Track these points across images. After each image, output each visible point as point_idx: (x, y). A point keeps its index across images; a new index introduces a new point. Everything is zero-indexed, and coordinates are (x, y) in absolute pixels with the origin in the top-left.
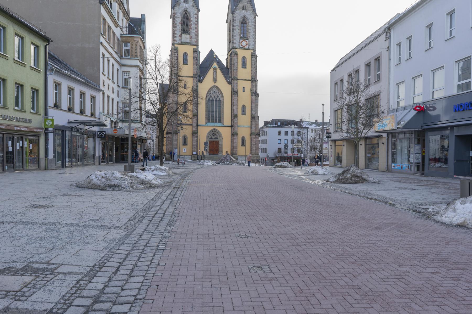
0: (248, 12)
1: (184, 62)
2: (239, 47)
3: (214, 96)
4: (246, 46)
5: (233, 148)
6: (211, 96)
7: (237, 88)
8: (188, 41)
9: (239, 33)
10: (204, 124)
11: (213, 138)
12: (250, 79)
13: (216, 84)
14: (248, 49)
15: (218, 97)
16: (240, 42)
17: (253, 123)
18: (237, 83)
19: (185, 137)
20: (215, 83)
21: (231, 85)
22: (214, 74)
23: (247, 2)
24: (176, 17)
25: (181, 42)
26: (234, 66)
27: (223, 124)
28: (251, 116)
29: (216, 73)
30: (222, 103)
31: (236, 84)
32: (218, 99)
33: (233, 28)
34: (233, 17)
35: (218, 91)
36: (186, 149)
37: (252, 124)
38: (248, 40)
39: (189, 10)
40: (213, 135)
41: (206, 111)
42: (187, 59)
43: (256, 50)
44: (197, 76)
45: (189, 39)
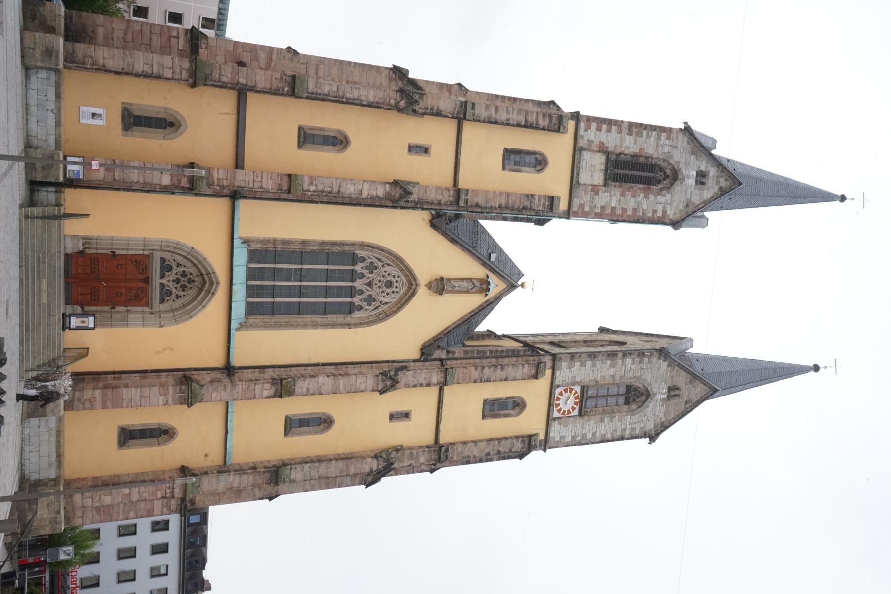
0: (663, 406)
1: (512, 157)
2: (557, 383)
3: (369, 284)
4: (559, 411)
5: (106, 387)
6: (372, 268)
7: (407, 386)
8: (584, 178)
9: (604, 377)
10: (241, 231)
11: (162, 276)
12: (443, 440)
13: (422, 291)
14: (549, 419)
15: (370, 300)
16: (574, 384)
17: (251, 477)
18: (428, 385)
19: (172, 124)
20: (429, 286)
21: (417, 356)
22: (465, 284)
24: (659, 138)
25: (582, 149)
26: (495, 366)
27: (242, 326)
28: (284, 465)
29: (467, 291)
30: (340, 318)
31: (424, 382)
32: (357, 300)
33: (620, 355)
34: (652, 355)
35: (392, 299)
36: (97, 122)
37: (240, 470)
38: (580, 414)
39: (677, 187)
40: (184, 274)
41: (304, 242)
42: (523, 169)
43: (545, 451)
44: (462, 204)
45: (588, 181)
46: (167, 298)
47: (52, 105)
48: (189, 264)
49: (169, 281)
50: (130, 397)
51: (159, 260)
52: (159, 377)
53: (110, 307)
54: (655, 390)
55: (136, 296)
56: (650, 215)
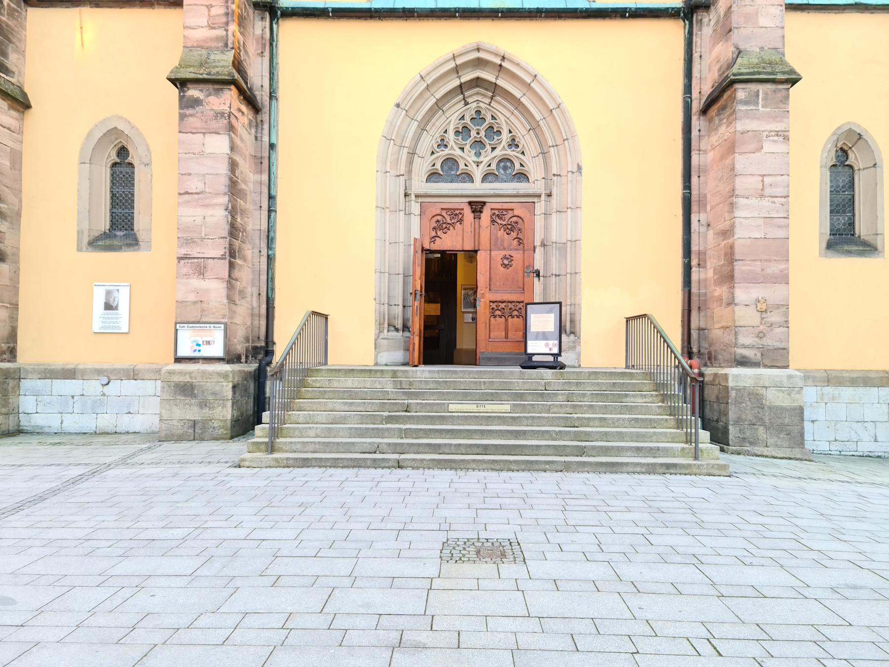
11: (468, 177)
36: (123, 298)
46: (517, 166)
47: (93, 387)
48: (438, 123)
49: (478, 164)
50: (761, 222)
51: (430, 184)
52: (701, 171)
53: (536, 280)
55: (510, 228)
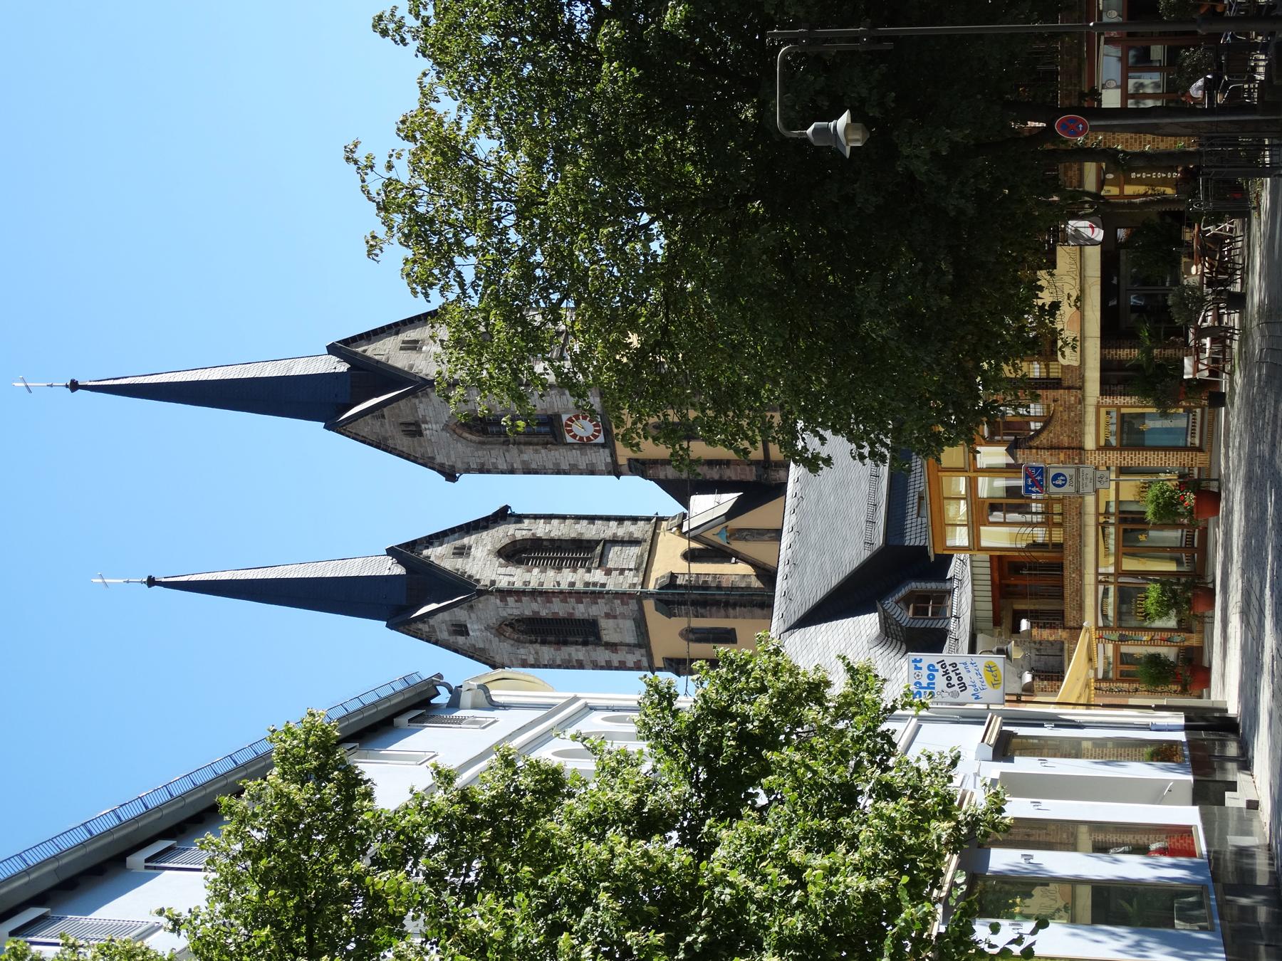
0: (424, 416)
23: (378, 417)
39: (493, 621)
45: (620, 621)
54: (445, 435)
56: (524, 599)
